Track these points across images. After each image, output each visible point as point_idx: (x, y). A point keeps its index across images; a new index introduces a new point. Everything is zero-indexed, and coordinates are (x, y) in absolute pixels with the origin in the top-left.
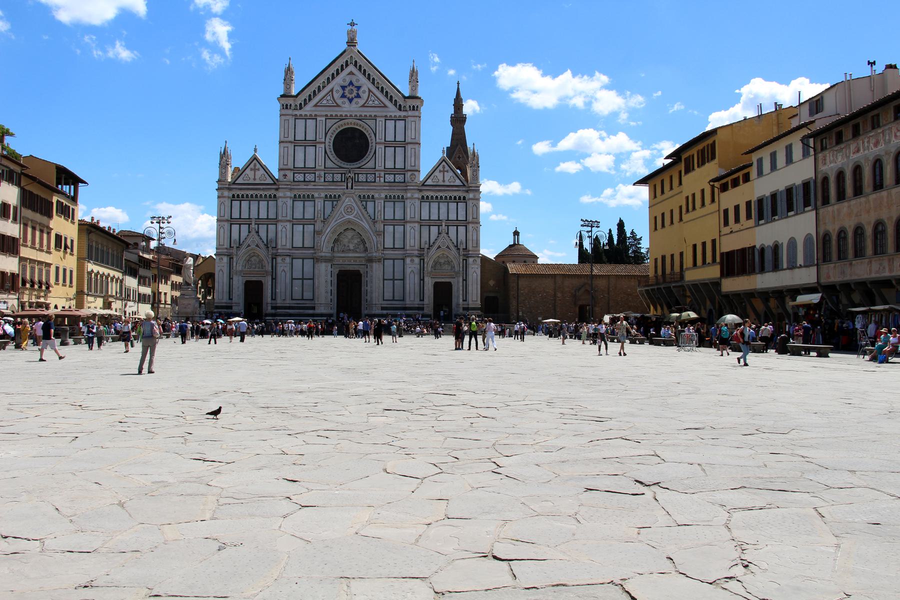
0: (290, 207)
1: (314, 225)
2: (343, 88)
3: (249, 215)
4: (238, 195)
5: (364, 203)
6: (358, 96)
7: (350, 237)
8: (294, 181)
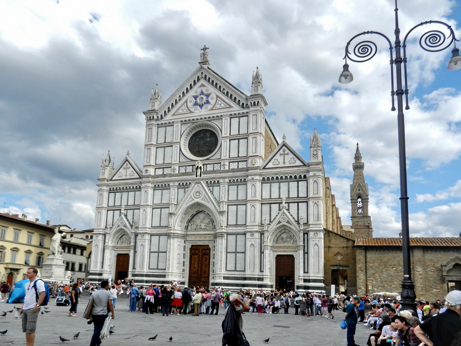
0: (151, 195)
1: (168, 208)
2: (195, 97)
3: (121, 203)
4: (113, 188)
5: (211, 188)
6: (208, 102)
7: (202, 218)
8: (155, 174)
